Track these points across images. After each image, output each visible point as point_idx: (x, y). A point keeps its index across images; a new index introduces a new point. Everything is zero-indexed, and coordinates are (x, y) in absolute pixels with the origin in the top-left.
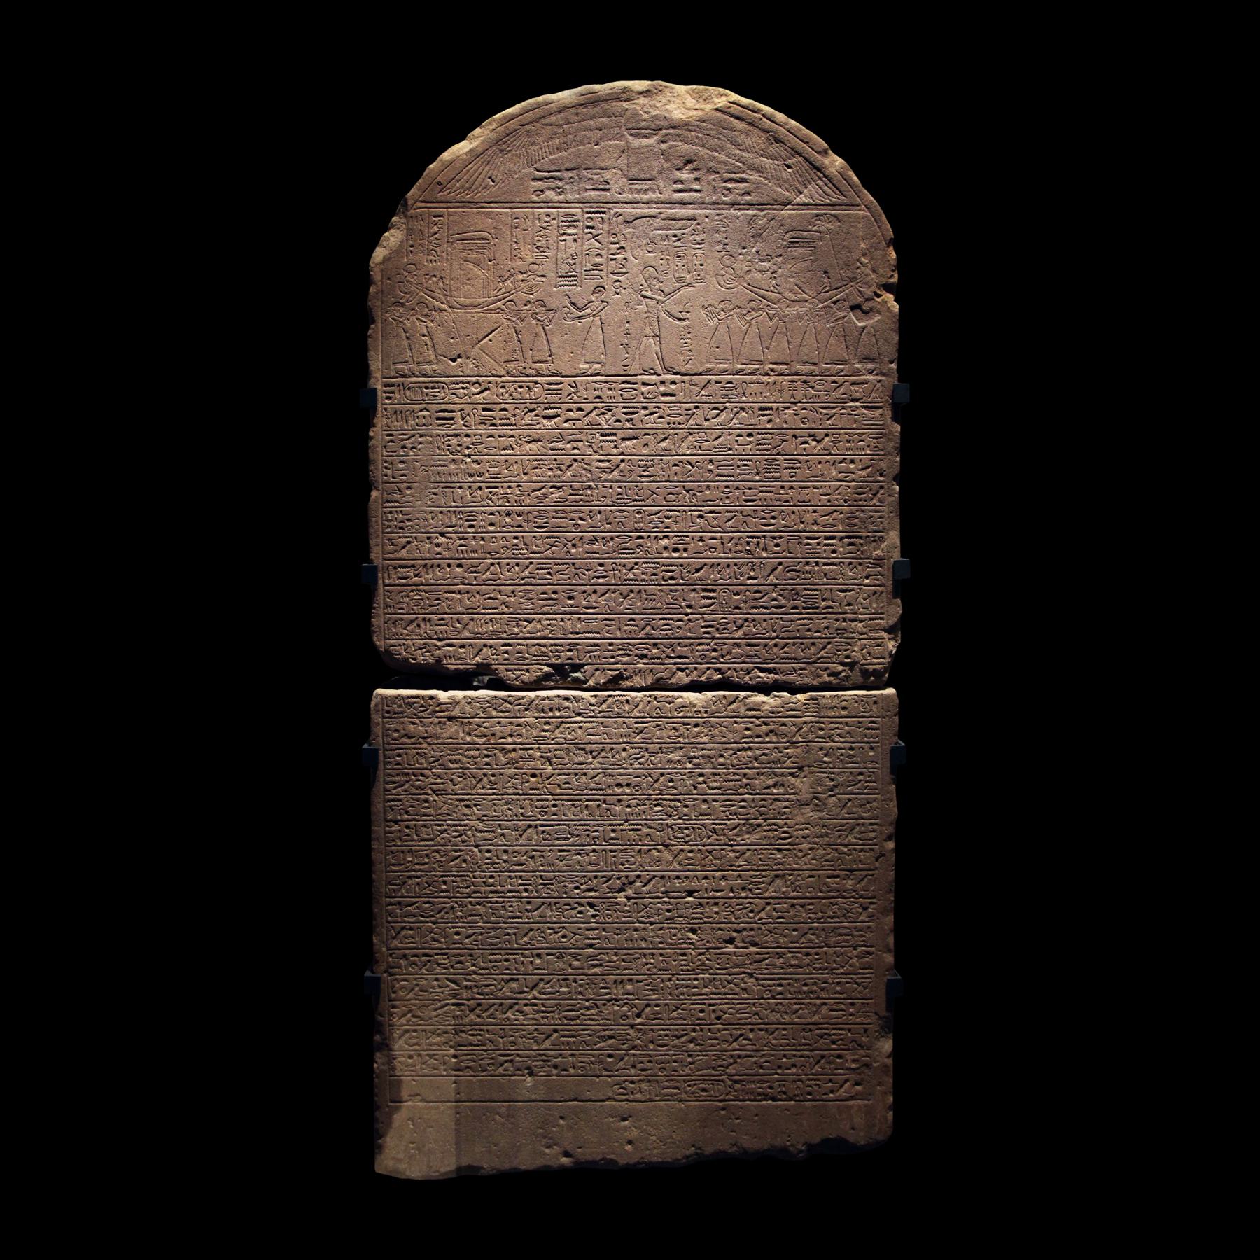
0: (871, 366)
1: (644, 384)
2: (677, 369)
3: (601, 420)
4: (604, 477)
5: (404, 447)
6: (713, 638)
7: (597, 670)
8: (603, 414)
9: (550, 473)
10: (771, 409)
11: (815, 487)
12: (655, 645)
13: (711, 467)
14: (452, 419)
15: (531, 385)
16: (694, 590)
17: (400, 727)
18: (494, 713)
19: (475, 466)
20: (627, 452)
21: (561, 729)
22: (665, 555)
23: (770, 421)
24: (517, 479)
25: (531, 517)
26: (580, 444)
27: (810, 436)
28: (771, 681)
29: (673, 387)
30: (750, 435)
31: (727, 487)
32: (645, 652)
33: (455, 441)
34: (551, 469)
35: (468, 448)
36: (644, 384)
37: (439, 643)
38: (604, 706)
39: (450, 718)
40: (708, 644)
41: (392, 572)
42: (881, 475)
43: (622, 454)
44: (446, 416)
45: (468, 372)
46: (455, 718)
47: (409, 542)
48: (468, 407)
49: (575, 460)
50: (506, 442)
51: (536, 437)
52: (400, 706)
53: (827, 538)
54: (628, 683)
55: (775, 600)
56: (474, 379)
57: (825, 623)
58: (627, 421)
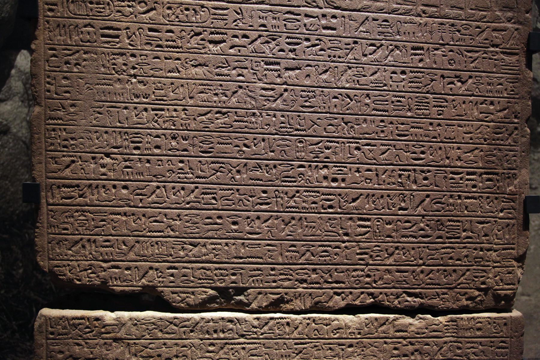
0: (510, 14)
1: (307, 16)
2: (338, 4)
3: (266, 48)
4: (268, 105)
5: (67, 63)
6: (367, 265)
7: (260, 293)
8: (268, 42)
9: (215, 98)
10: (422, 49)
11: (459, 126)
12: (314, 270)
13: (368, 101)
14: (117, 37)
15: (197, 8)
16: (351, 219)
17: (65, 349)
18: (160, 335)
20: (290, 81)
21: (225, 350)
22: (325, 184)
23: (421, 60)
24: (183, 102)
25: (196, 141)
26: (245, 71)
27: (456, 77)
28: (417, 305)
29: (334, 21)
30: (403, 73)
31: (382, 121)
32: (305, 277)
33: (120, 60)
34: (216, 94)
35: (134, 68)
36: (307, 16)
37: (104, 265)
38: (266, 328)
39: (116, 340)
40: (363, 270)
41: (56, 191)
42: (516, 117)
43: (285, 83)
44: (111, 33)
46: (121, 339)
47: (73, 162)
49: (240, 87)
50: (172, 64)
51: (201, 61)
52: (65, 328)
53: (468, 174)
54: (289, 307)
55: (422, 229)
57: (465, 252)
58: (291, 51)
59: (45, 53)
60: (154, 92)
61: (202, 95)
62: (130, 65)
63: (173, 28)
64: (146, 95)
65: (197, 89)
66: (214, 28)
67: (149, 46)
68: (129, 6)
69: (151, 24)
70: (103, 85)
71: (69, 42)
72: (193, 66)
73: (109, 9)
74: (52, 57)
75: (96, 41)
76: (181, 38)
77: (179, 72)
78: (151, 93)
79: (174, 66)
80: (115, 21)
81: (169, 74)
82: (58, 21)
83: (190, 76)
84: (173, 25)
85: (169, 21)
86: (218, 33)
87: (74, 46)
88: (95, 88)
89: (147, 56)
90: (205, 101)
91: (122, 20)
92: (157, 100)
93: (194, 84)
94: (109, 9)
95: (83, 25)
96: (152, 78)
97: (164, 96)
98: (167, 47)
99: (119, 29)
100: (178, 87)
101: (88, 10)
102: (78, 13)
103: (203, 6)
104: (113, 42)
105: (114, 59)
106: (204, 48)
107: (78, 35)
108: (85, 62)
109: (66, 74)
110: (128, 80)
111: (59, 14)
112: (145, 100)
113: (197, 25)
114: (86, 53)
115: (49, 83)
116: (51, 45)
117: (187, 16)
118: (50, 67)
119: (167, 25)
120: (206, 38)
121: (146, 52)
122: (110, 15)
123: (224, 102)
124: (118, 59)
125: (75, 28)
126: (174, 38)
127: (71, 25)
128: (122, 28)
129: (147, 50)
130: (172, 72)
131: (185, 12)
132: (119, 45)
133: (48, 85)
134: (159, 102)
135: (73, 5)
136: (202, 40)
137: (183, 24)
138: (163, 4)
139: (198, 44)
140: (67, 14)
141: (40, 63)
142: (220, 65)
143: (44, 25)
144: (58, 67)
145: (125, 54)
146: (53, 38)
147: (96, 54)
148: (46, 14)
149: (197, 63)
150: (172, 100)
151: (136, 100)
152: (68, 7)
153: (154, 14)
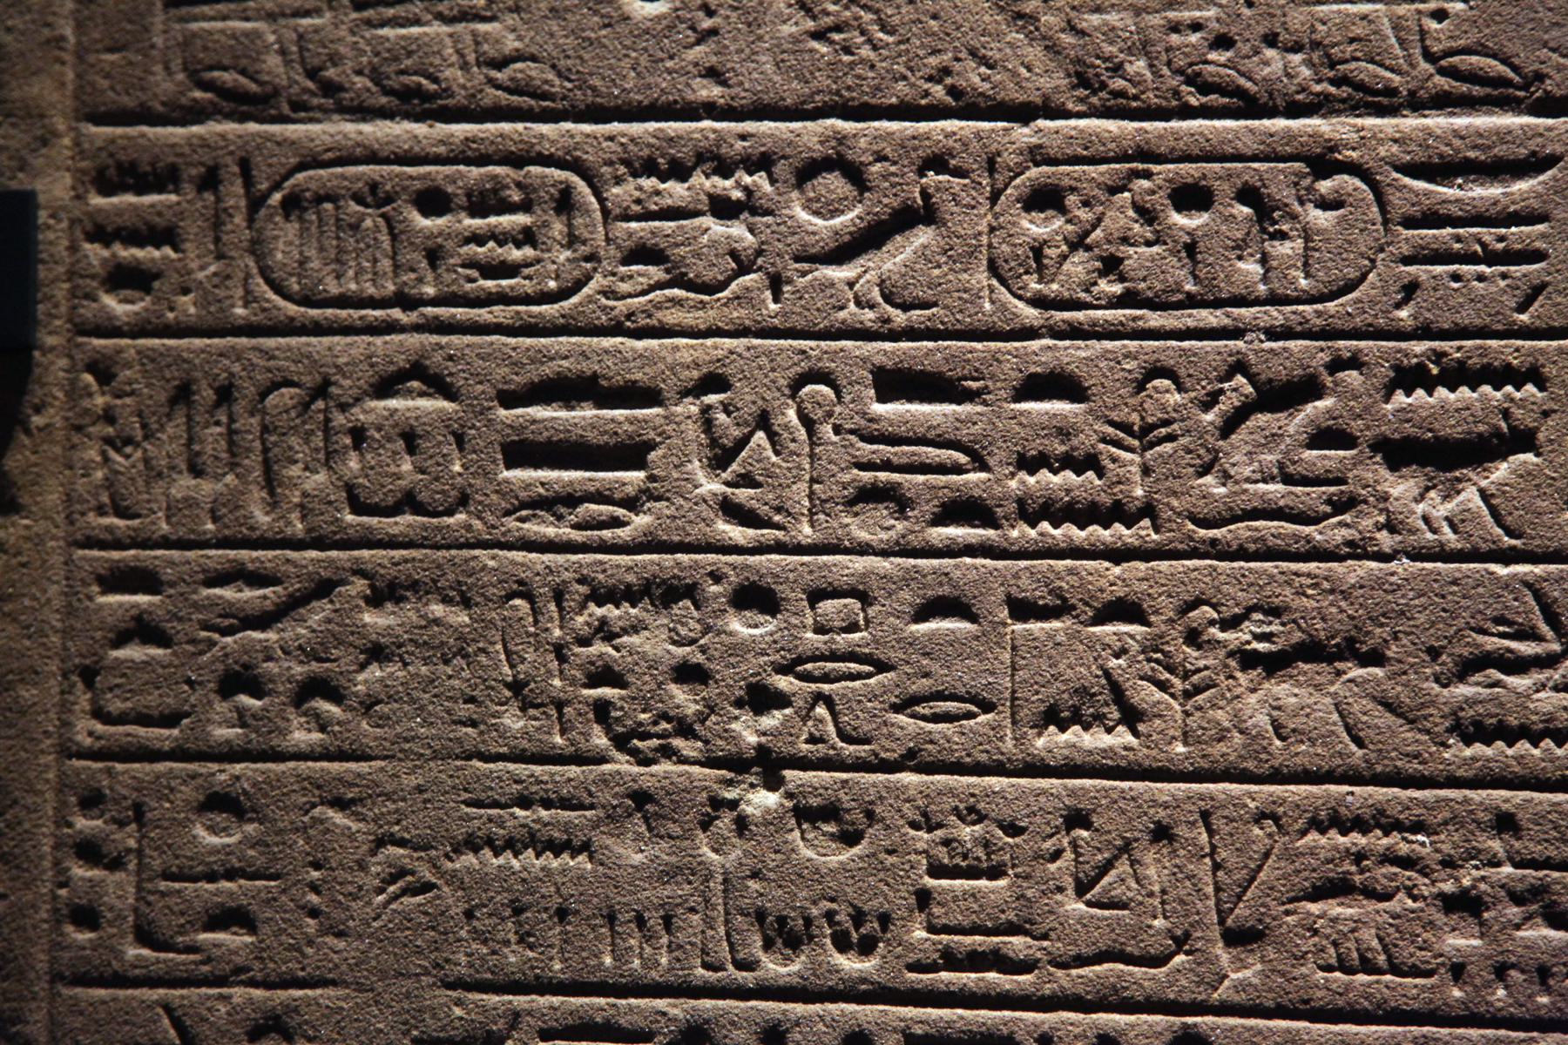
5: (240, 679)
9: (1461, 941)
14: (631, 453)
15: (1278, 180)
19: (815, 850)
33: (652, 641)
34: (1465, 904)
35: (761, 699)
44: (587, 429)
45: (762, 75)
48: (761, 364)
50: (1067, 650)
51: (1329, 618)
56: (810, 134)
59: (69, 611)
60: (924, 898)
61: (1335, 908)
62: (731, 678)
63: (1073, 354)
64: (858, 918)
65: (1290, 855)
66: (1424, 332)
67: (882, 512)
68: (723, 208)
69: (894, 336)
70: (512, 845)
71: (262, 518)
72: (1248, 660)
73: (572, 240)
74: (121, 640)
75: (463, 501)
76: (1146, 435)
77: (1132, 717)
78: (901, 900)
79: (1087, 673)
80: (616, 329)
81: (1052, 742)
82: (179, 359)
83: (1230, 750)
84: (1075, 332)
85: (1039, 302)
86: (1457, 375)
87: (299, 545)
88: (453, 878)
89: (865, 598)
90: (1368, 967)
91: (672, 317)
92: (951, 960)
93: (1260, 817)
94: (572, 240)
95: (366, 376)
96: (908, 778)
97: (1012, 929)
98: (1030, 511)
99: (650, 396)
100: (1126, 848)
101: (408, 256)
102: (334, 289)
103: (1323, 162)
104: (599, 497)
105: (604, 631)
106: (1342, 505)
107: (330, 457)
108: (375, 671)
109: (223, 774)
110: (717, 803)
111: (188, 305)
112: (851, 965)
113: (1275, 315)
114: (384, 594)
115: (89, 851)
116: (118, 545)
117: (1191, 249)
118: (108, 719)
119: (1029, 333)
120: (1356, 426)
121: (860, 563)
122: (579, 285)
123: (1544, 973)
124: (635, 629)
125: (306, 406)
126: (1085, 441)
127: (275, 386)
128: (668, 387)
129: (863, 549)
130: (1077, 718)
131: (1178, 219)
132: (641, 521)
133: (79, 871)
134: (968, 978)
135: (292, 228)
136: (1326, 436)
137: (1155, 319)
138: (991, 166)
139: (1288, 479)
140: (249, 298)
141: (27, 694)
142: (1492, 643)
143: (75, 393)
144: (170, 720)
145: (690, 592)
146: (135, 494)
147: (466, 603)
148: (88, 311)
149: (1284, 635)
150: (1081, 961)
151: (775, 968)
152: (257, 248)
153: (922, 253)
